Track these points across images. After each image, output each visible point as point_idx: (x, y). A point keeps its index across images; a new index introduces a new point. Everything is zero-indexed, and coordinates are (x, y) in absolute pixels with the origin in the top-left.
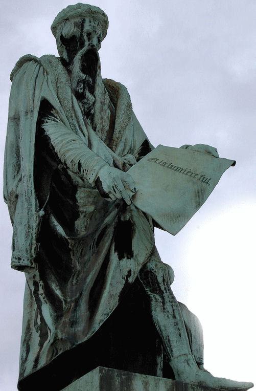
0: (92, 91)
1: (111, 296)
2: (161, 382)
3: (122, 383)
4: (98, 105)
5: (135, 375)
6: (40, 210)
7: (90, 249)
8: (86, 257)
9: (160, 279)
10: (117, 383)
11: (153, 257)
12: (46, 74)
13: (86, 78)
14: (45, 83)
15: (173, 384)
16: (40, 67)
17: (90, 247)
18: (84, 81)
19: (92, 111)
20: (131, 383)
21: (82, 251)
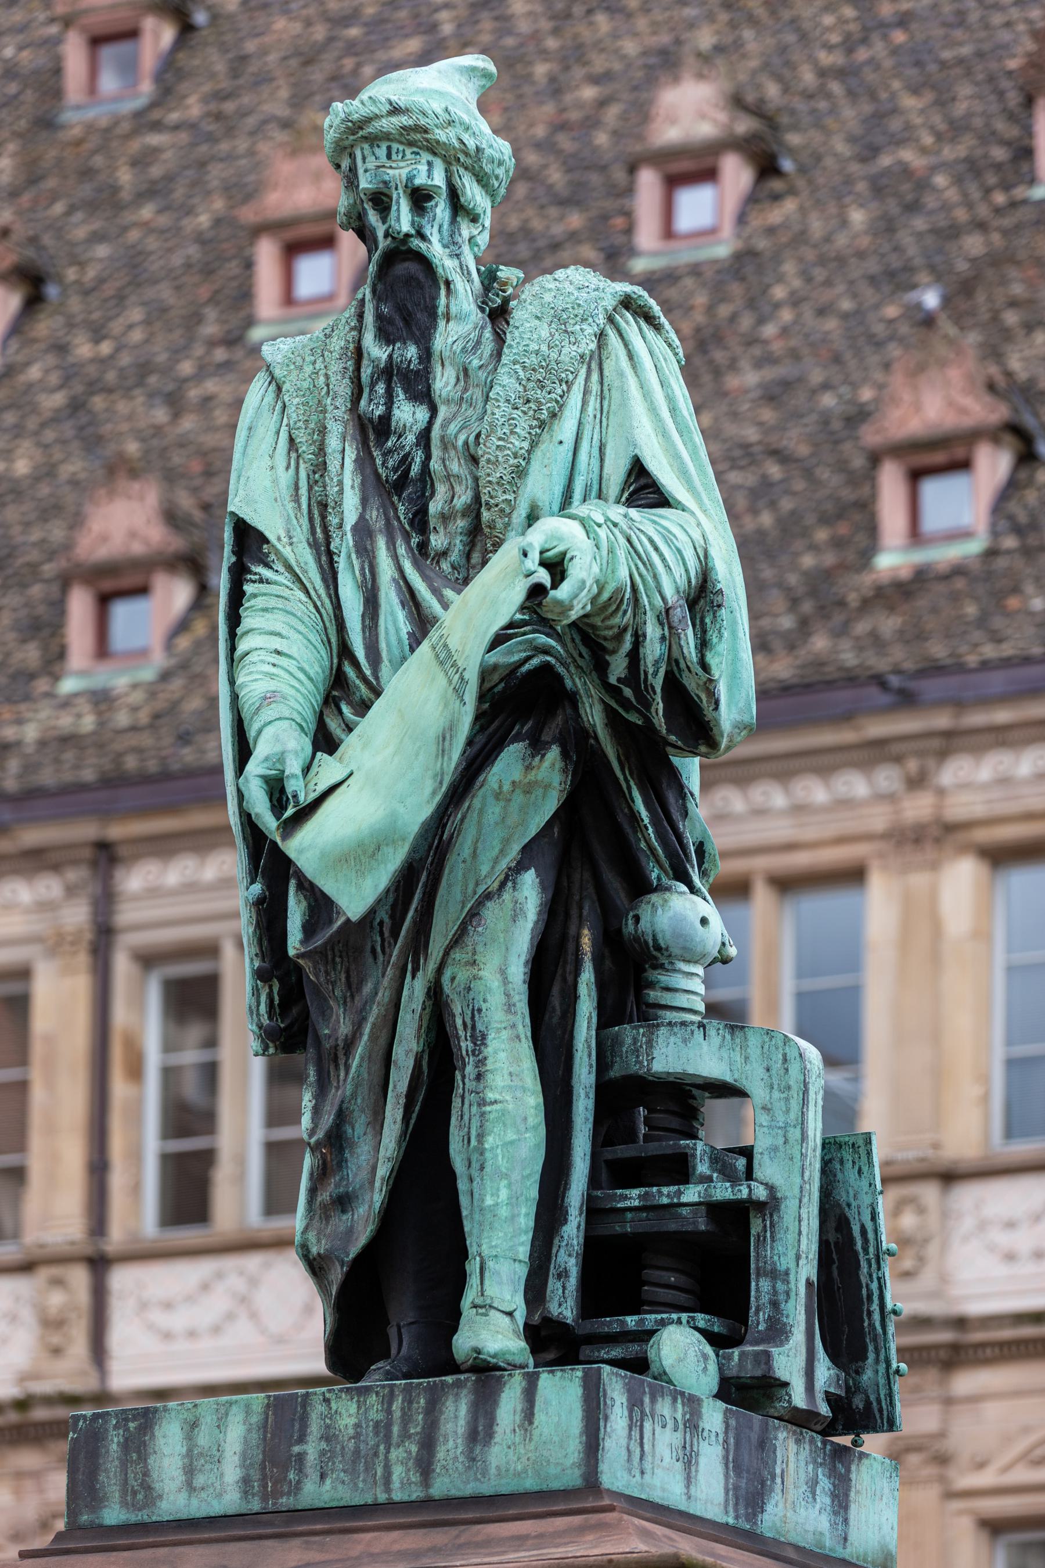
0: (423, 395)
1: (398, 1096)
2: (234, 1409)
3: (126, 1446)
4: (436, 433)
5: (166, 1409)
6: (253, 882)
7: (375, 958)
8: (368, 988)
9: (459, 1022)
10: (114, 1446)
11: (457, 955)
12: (280, 404)
13: (390, 356)
14: (270, 437)
15: (268, 1406)
16: (270, 383)
17: (373, 951)
18: (388, 372)
19: (415, 469)
20: (153, 1436)
21: (348, 978)
